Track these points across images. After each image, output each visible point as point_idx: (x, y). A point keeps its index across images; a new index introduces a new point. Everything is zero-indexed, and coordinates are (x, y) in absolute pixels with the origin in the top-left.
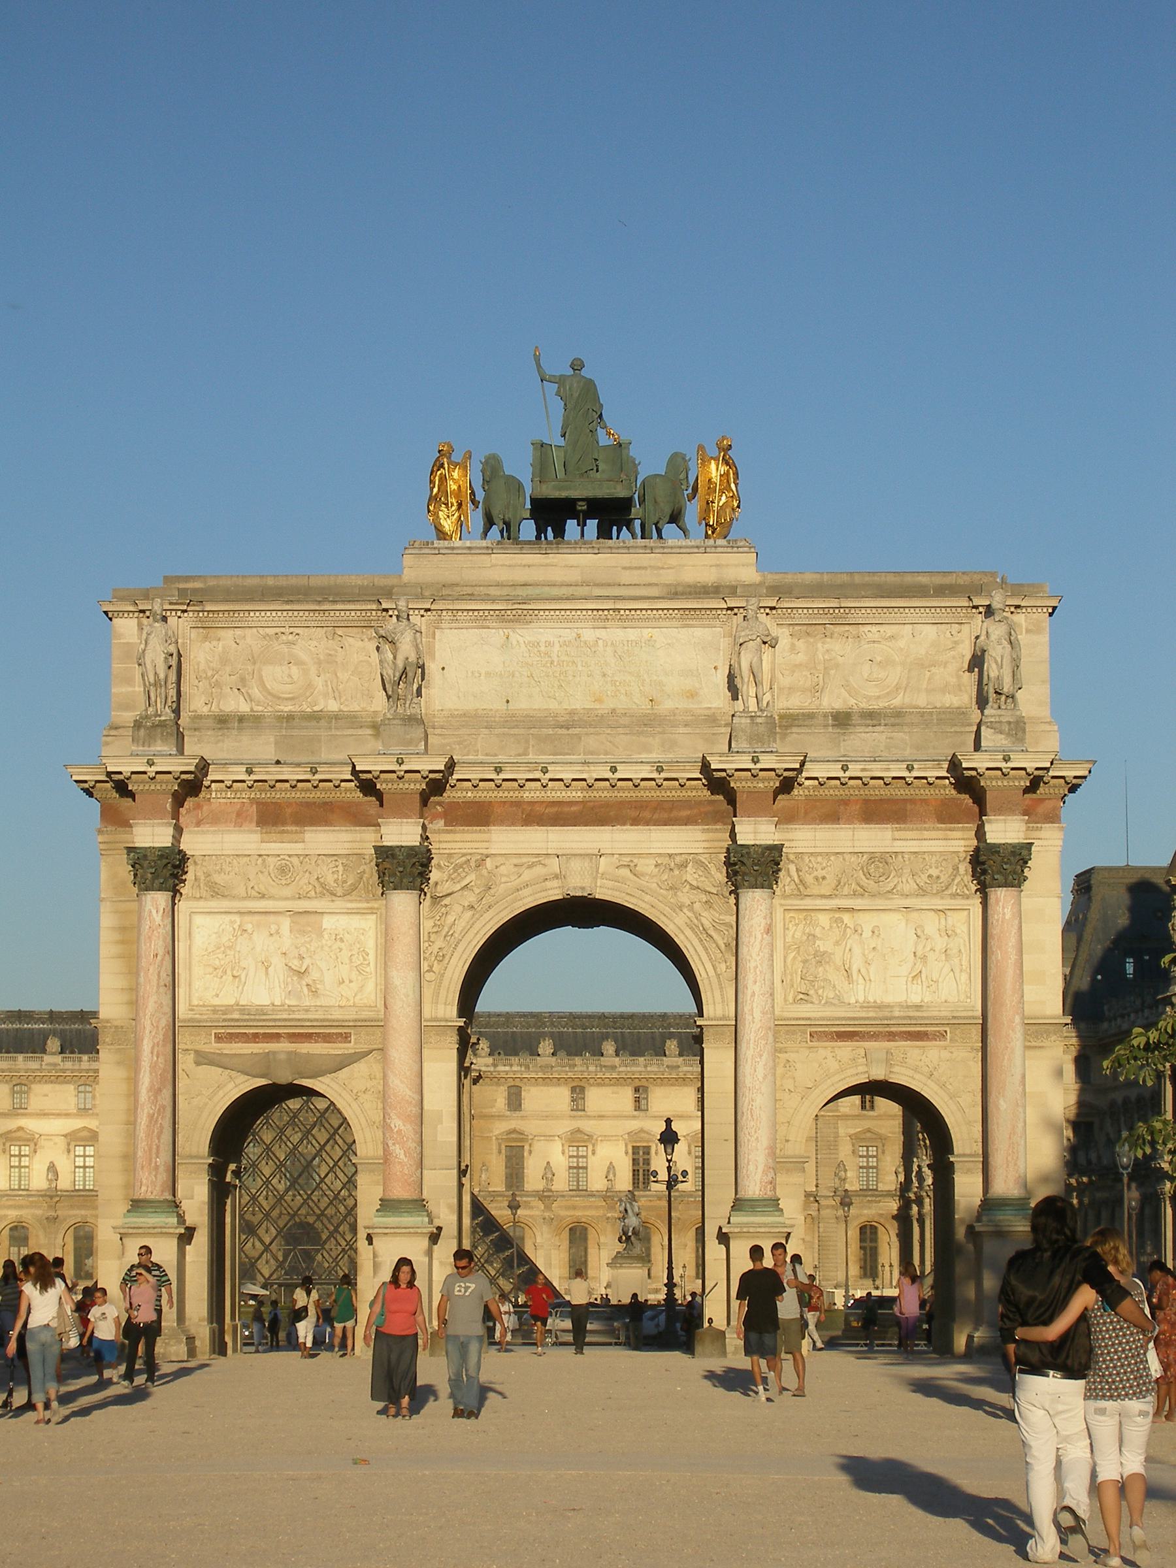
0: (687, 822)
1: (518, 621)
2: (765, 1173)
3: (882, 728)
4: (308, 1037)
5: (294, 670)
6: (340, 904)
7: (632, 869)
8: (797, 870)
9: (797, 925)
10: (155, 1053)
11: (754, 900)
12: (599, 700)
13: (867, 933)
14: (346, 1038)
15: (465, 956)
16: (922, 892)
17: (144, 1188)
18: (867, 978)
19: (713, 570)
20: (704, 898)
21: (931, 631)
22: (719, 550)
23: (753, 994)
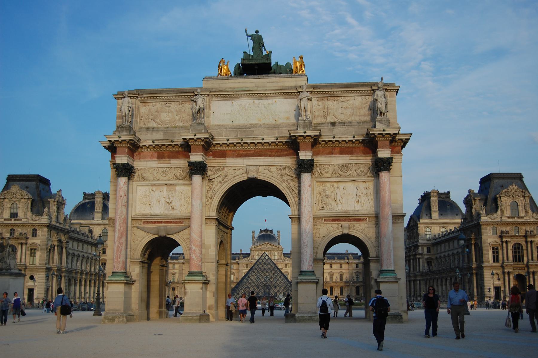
0: (286, 155)
1: (236, 98)
2: (309, 262)
3: (345, 126)
4: (171, 222)
5: (170, 114)
6: (181, 182)
7: (269, 169)
8: (320, 170)
9: (320, 186)
11: (306, 177)
12: (260, 121)
13: (342, 189)
14: (182, 222)
15: (218, 197)
16: (359, 175)
17: (115, 268)
18: (342, 202)
19: (294, 82)
20: (291, 178)
21: (360, 98)
22: (296, 76)
23: (305, 206)
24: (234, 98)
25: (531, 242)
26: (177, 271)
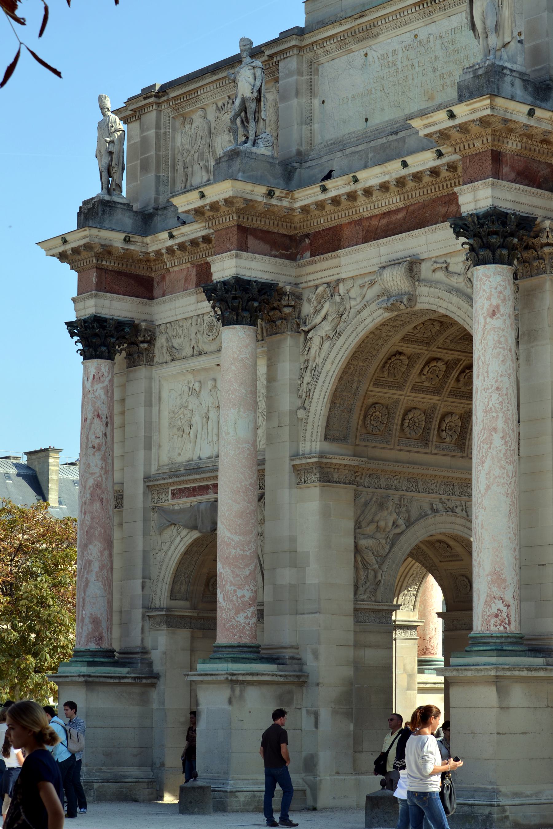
1: (369, 37)
2: (487, 604)
10: (83, 511)
15: (325, 389)
24: (364, 39)
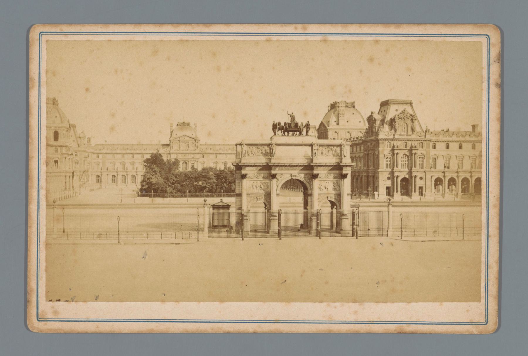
25: (415, 154)
26: (101, 161)
